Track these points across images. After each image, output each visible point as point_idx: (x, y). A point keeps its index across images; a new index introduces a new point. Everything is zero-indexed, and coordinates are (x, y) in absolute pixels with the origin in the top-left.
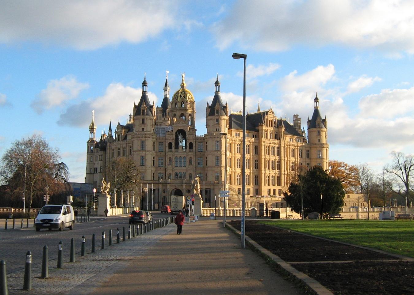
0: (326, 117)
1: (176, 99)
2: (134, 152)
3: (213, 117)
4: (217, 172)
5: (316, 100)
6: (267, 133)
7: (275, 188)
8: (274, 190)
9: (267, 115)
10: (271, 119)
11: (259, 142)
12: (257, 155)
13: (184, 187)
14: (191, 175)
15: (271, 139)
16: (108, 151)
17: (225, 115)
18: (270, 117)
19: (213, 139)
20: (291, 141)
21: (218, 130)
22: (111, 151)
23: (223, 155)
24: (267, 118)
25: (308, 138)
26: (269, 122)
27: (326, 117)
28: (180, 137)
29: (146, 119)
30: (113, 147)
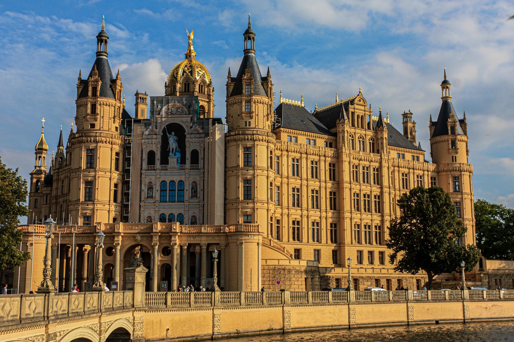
0: (464, 115)
1: (175, 77)
2: (74, 174)
3: (238, 98)
4: (247, 212)
5: (445, 84)
6: (353, 140)
7: (371, 249)
8: (371, 253)
9: (352, 104)
10: (361, 113)
11: (338, 156)
12: (334, 182)
13: (156, 239)
14: (196, 220)
15: (361, 153)
16: (55, 185)
17: (265, 94)
18: (358, 109)
19: (240, 143)
20: (399, 157)
21: (250, 125)
22: (60, 184)
23: (259, 176)
24: (353, 110)
25: (432, 156)
26: (356, 118)
27: (464, 115)
28: (173, 143)
29: (100, 105)
30: (62, 177)
